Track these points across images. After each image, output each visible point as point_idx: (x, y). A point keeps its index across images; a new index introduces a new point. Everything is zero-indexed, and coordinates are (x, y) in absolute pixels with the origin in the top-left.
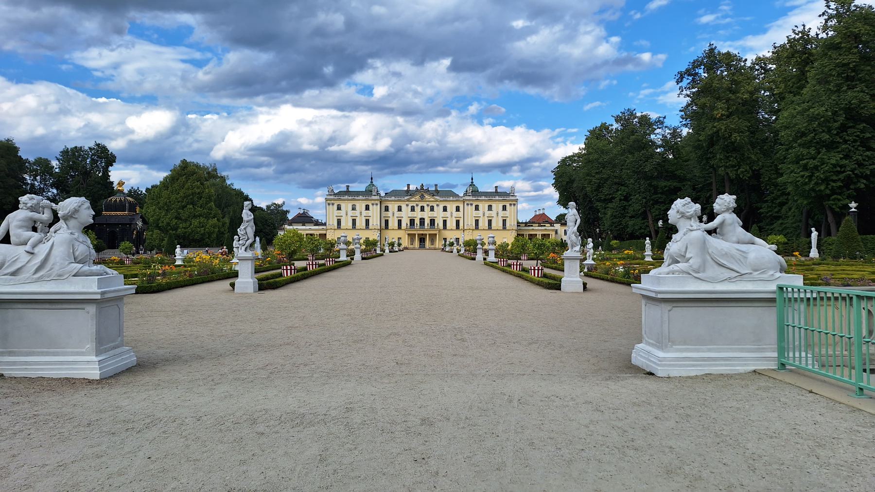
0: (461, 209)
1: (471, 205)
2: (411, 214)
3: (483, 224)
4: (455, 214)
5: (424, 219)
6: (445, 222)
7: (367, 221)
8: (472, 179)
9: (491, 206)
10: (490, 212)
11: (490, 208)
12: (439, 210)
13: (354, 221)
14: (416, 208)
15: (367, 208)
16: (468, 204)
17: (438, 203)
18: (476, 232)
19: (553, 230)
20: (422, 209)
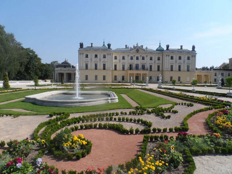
0: (161, 59)
2: (130, 61)
3: (176, 68)
6: (151, 67)
7: (104, 65)
8: (160, 44)
10: (180, 60)
11: (180, 58)
14: (133, 58)
15: (104, 57)
16: (166, 55)
20: (137, 58)
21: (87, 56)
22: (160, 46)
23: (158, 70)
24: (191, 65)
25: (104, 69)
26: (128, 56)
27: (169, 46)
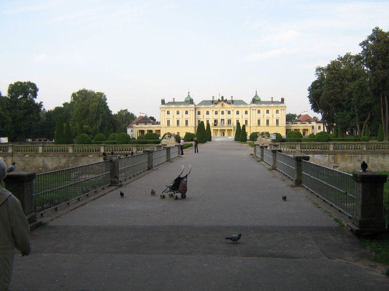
0: (249, 113)
1: (255, 110)
2: (216, 117)
4: (244, 115)
5: (224, 120)
10: (268, 115)
11: (268, 112)
12: (234, 113)
13: (178, 122)
15: (187, 113)
18: (259, 128)
19: (310, 126)
20: (223, 113)
21: (168, 113)
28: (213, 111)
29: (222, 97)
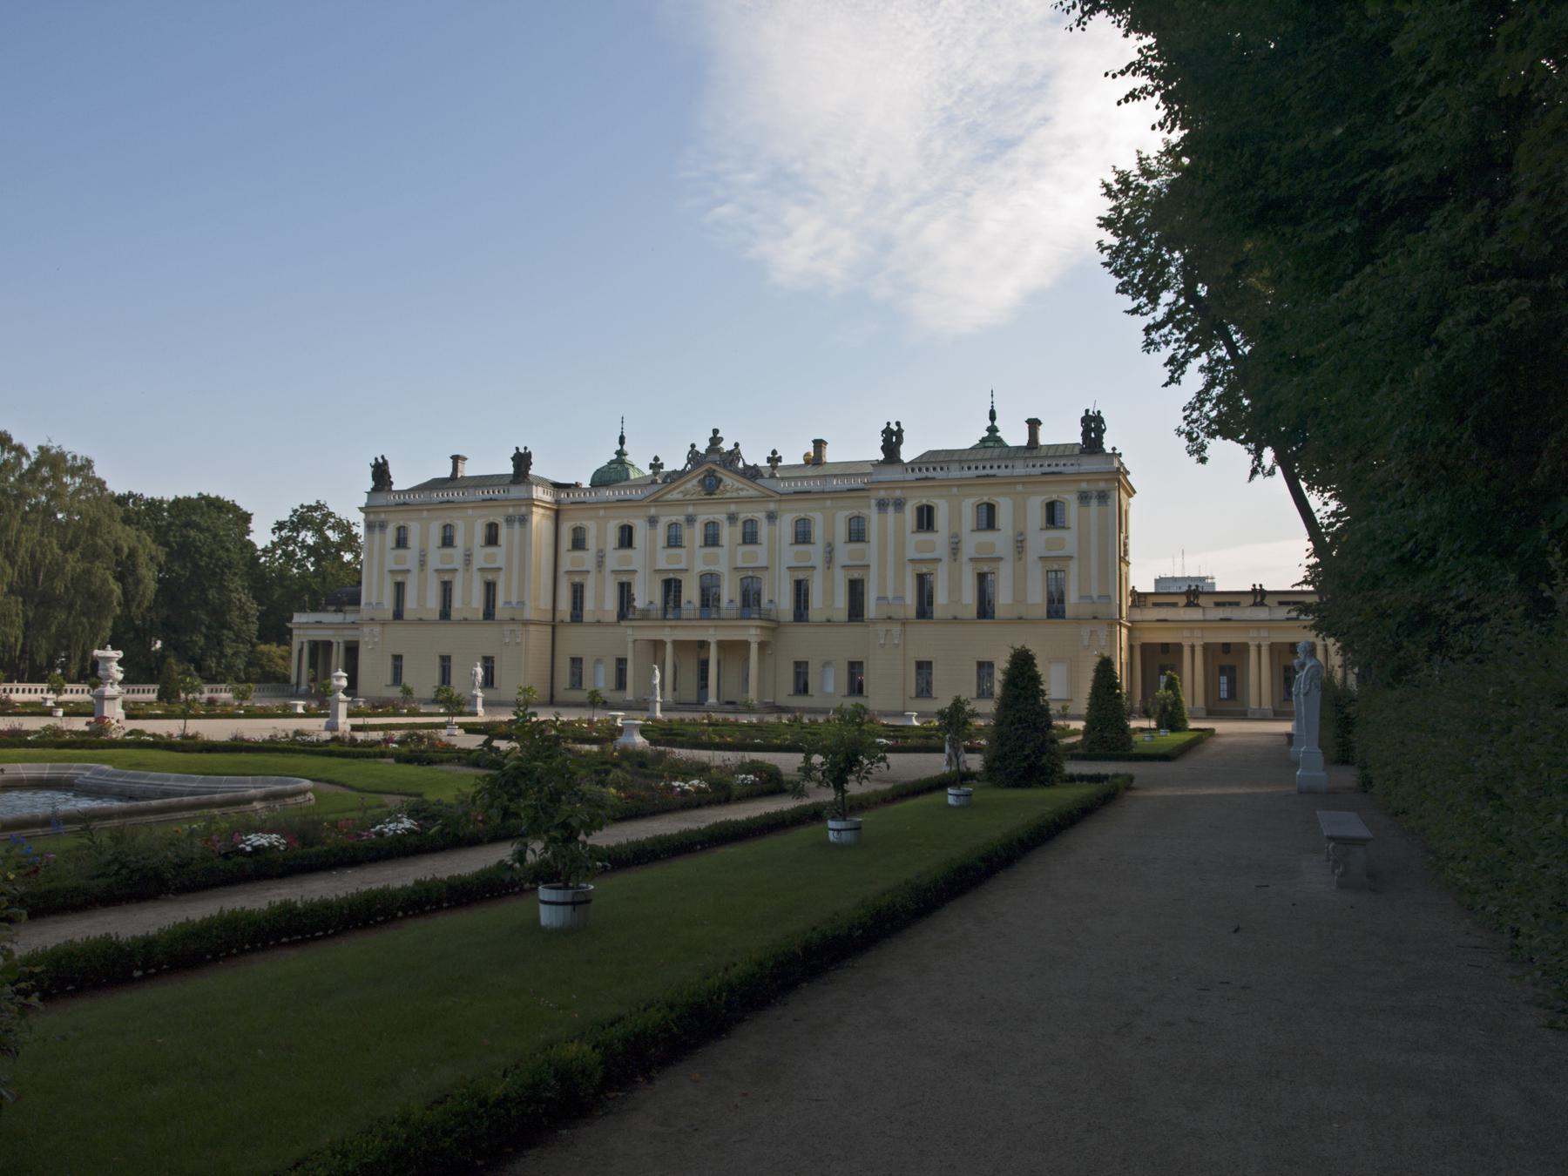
2: (666, 560)
6: (801, 591)
9: (991, 509)
10: (987, 537)
11: (988, 517)
13: (447, 588)
14: (686, 533)
15: (492, 538)
16: (882, 505)
17: (772, 506)
20: (712, 540)
21: (401, 542)
22: (992, 430)
23: (856, 610)
24: (1073, 567)
25: (489, 614)
26: (653, 521)
27: (899, 433)
28: (653, 521)
29: (715, 440)
